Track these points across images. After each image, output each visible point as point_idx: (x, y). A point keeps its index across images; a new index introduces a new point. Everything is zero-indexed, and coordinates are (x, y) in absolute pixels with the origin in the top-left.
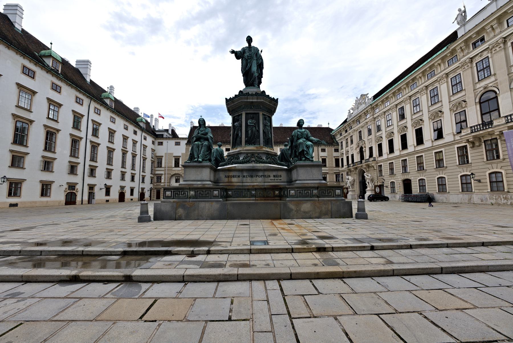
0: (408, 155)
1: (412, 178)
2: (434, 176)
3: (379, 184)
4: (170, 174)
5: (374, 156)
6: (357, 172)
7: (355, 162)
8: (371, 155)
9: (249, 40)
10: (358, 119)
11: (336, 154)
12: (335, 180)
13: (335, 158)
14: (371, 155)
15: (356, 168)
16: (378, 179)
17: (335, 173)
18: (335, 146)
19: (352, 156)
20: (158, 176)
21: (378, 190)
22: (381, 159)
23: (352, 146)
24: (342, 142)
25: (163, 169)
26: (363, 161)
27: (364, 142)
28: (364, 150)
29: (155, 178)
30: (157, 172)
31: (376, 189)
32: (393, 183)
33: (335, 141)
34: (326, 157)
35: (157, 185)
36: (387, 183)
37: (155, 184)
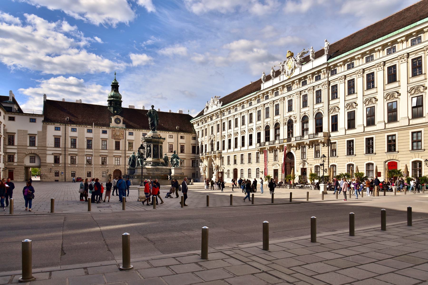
0: (237, 152)
3: (221, 171)
4: (25, 153)
5: (220, 149)
6: (208, 161)
7: (207, 151)
8: (218, 148)
9: (153, 107)
10: (211, 116)
11: (193, 142)
12: (191, 166)
13: (192, 145)
14: (218, 148)
15: (208, 157)
16: (221, 167)
17: (191, 159)
18: (193, 134)
19: (206, 145)
20: (10, 154)
21: (220, 175)
22: (223, 152)
23: (206, 137)
24: (199, 132)
25: (16, 147)
26: (212, 152)
27: (214, 136)
28: (214, 143)
29: (7, 157)
30: (8, 151)
31: (219, 175)
32: (228, 170)
33: (193, 130)
34: (185, 144)
35: (9, 165)
36: (225, 171)
37: (7, 164)
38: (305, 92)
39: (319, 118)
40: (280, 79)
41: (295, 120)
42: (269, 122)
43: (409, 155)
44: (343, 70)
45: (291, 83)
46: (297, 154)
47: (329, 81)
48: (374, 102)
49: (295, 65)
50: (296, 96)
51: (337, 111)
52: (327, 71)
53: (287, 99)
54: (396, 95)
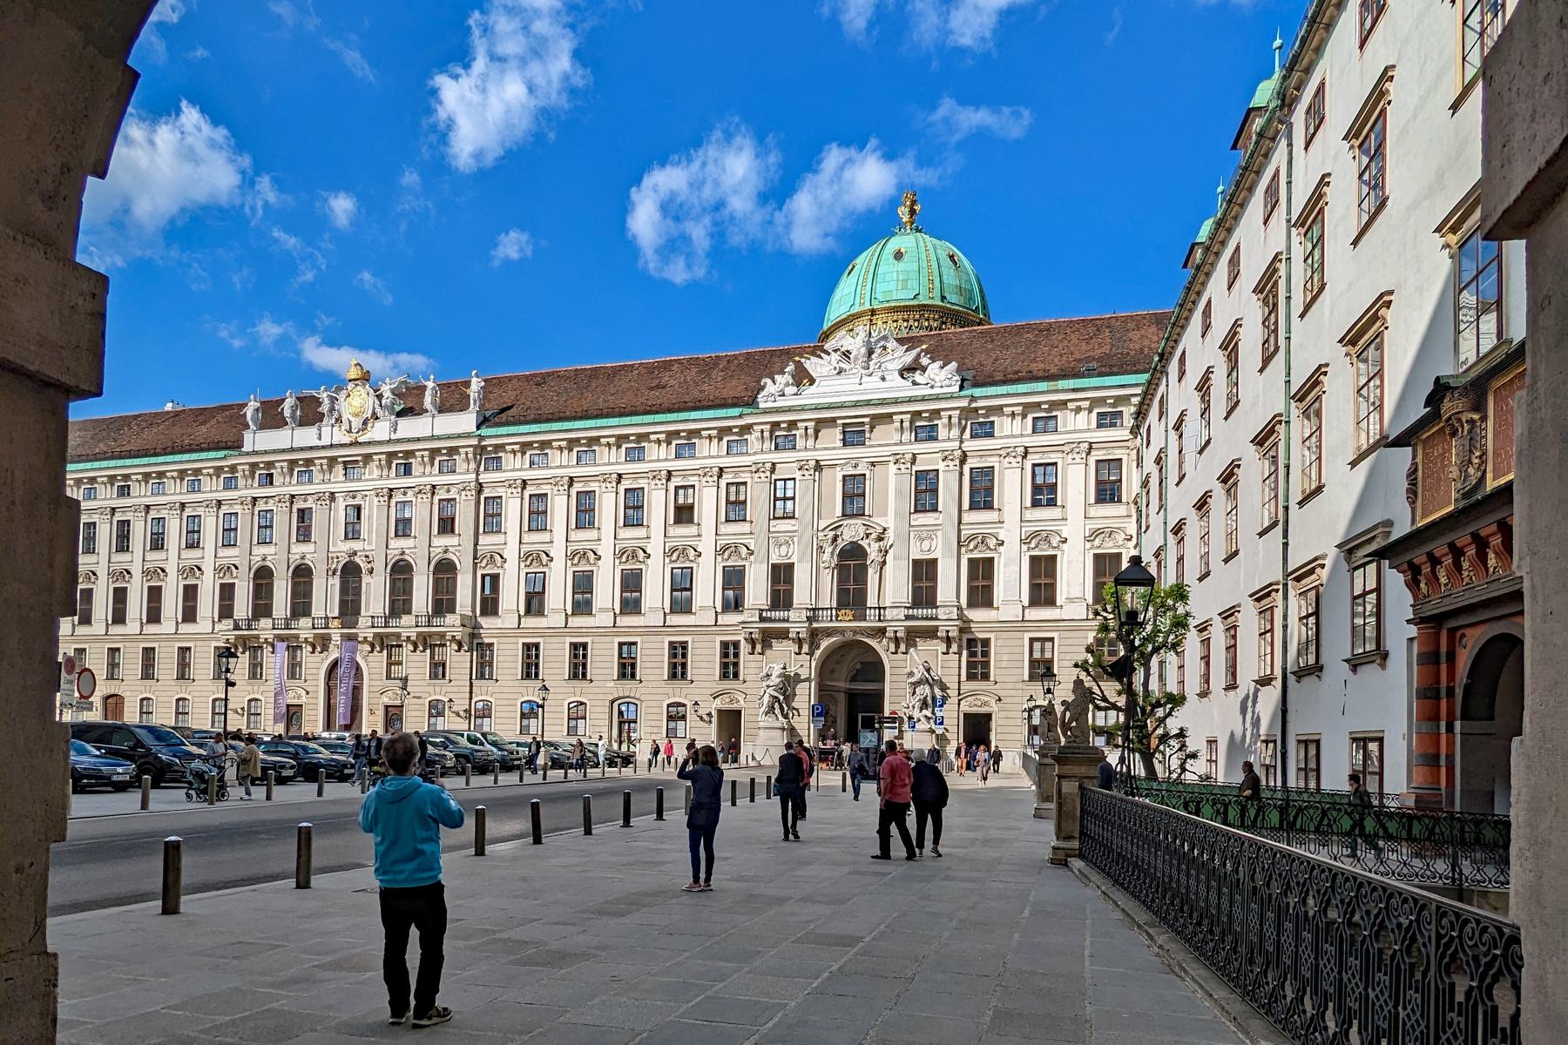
1: (128, 693)
2: (170, 694)
38: (405, 494)
39: (444, 571)
40: (320, 434)
41: (369, 566)
42: (269, 558)
43: (662, 690)
44: (518, 466)
45: (360, 458)
46: (372, 664)
47: (480, 484)
48: (592, 562)
49: (374, 408)
50: (376, 499)
51: (499, 565)
52: (475, 455)
53: (341, 499)
54: (641, 554)
